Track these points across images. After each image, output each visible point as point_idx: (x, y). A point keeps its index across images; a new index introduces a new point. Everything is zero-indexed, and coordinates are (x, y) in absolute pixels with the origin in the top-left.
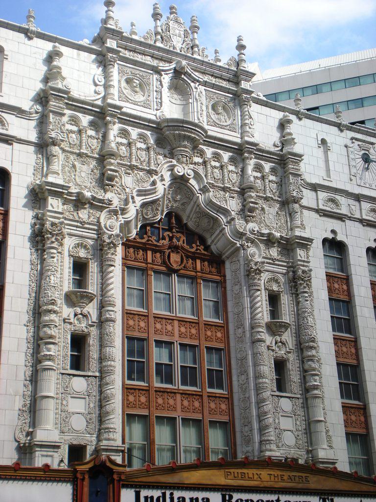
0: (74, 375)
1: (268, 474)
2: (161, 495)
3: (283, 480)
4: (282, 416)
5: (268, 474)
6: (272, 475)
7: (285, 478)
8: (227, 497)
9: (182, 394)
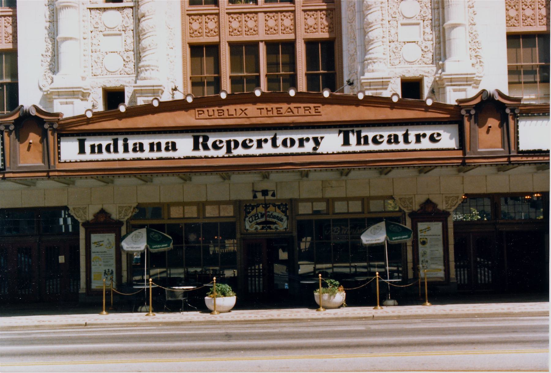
0: (105, 9)
1: (258, 109)
2: (112, 142)
3: (280, 114)
4: (402, 25)
5: (258, 109)
6: (263, 109)
7: (282, 111)
8: (201, 140)
9: (265, 12)
